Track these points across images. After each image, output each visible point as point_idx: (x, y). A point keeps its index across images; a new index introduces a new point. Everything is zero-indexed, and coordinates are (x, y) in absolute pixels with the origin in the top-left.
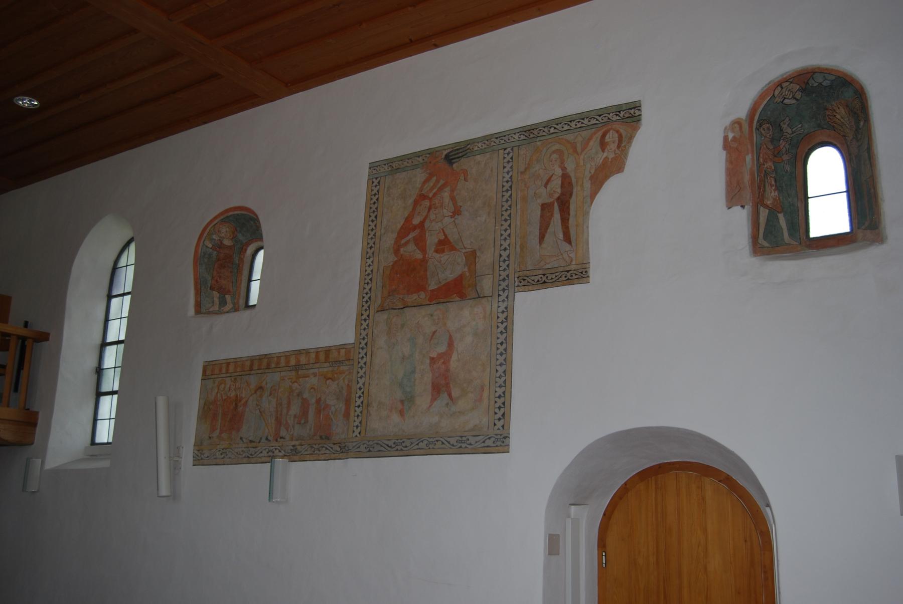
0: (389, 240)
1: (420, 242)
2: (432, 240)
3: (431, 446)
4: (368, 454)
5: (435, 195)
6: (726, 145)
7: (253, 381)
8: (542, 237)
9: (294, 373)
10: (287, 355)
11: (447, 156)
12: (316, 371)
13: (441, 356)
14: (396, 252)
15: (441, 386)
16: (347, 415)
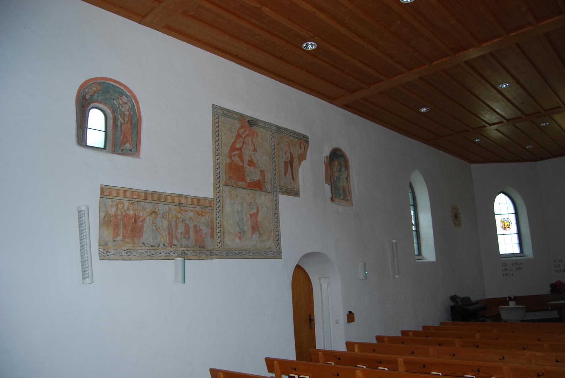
0: (226, 150)
1: (241, 156)
2: (246, 158)
5: (245, 137)
6: (325, 163)
7: (149, 207)
8: (285, 175)
10: (173, 196)
11: (248, 121)
12: (191, 209)
13: (254, 214)
15: (255, 228)
16: (212, 236)
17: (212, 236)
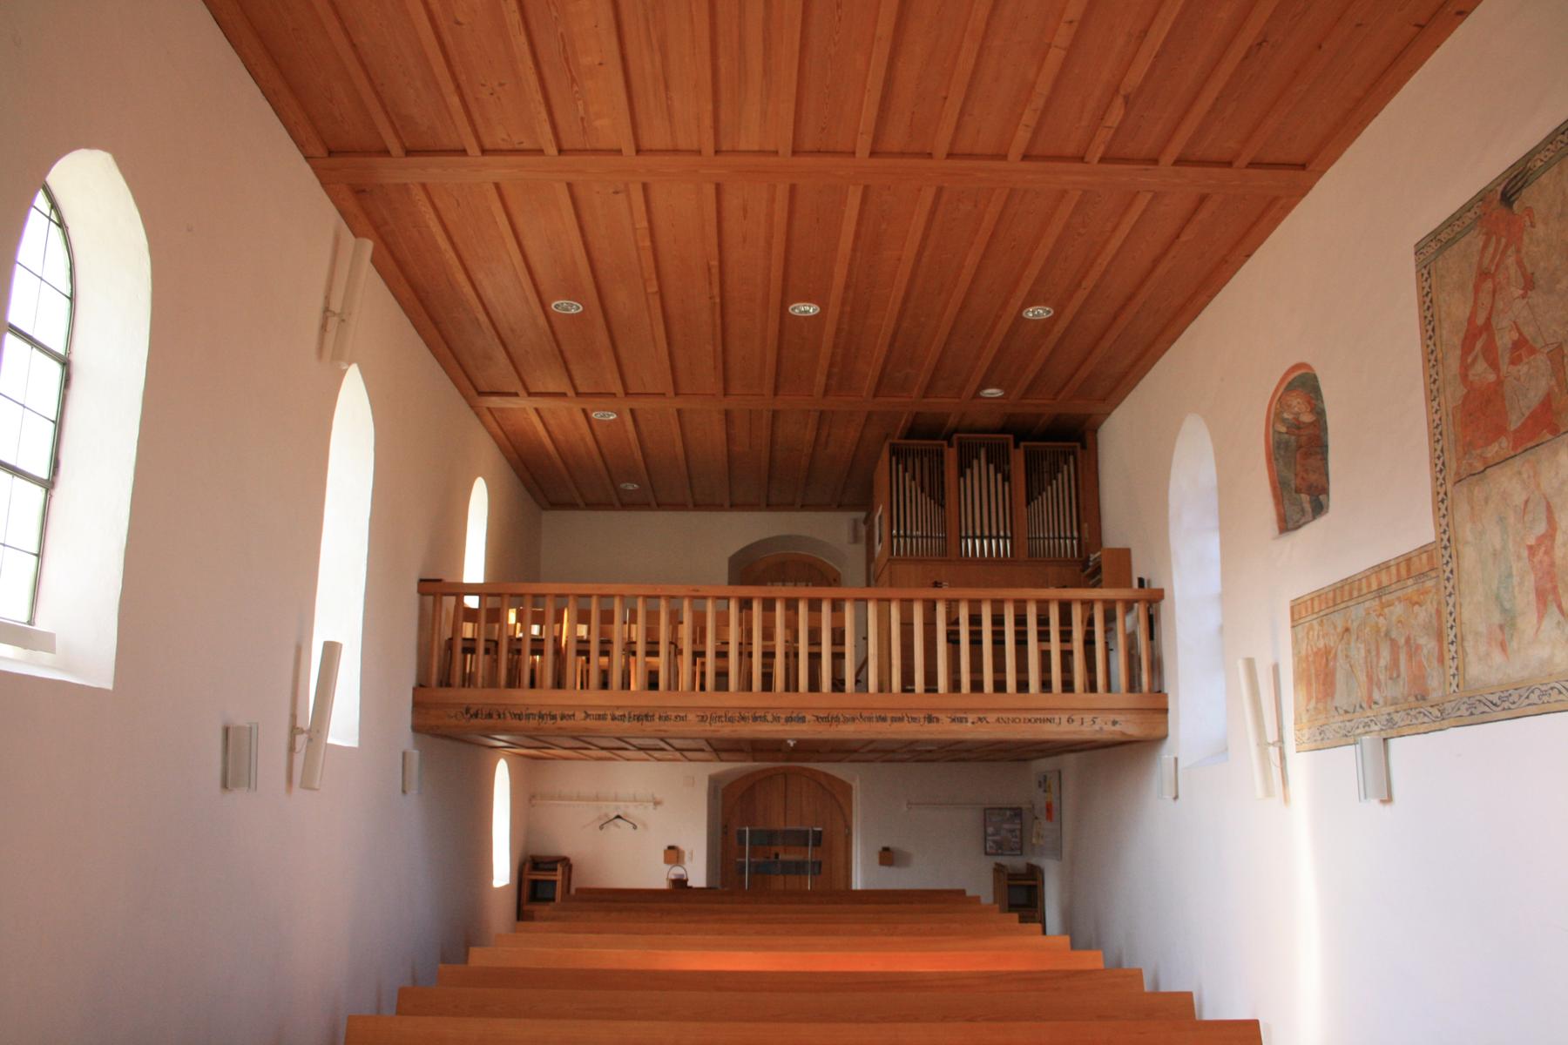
0: (1453, 362)
3: (1545, 699)
4: (1470, 719)
9: (1377, 602)
11: (1504, 194)
13: (1540, 540)
14: (1464, 377)
16: (1441, 660)
17: (1441, 660)
